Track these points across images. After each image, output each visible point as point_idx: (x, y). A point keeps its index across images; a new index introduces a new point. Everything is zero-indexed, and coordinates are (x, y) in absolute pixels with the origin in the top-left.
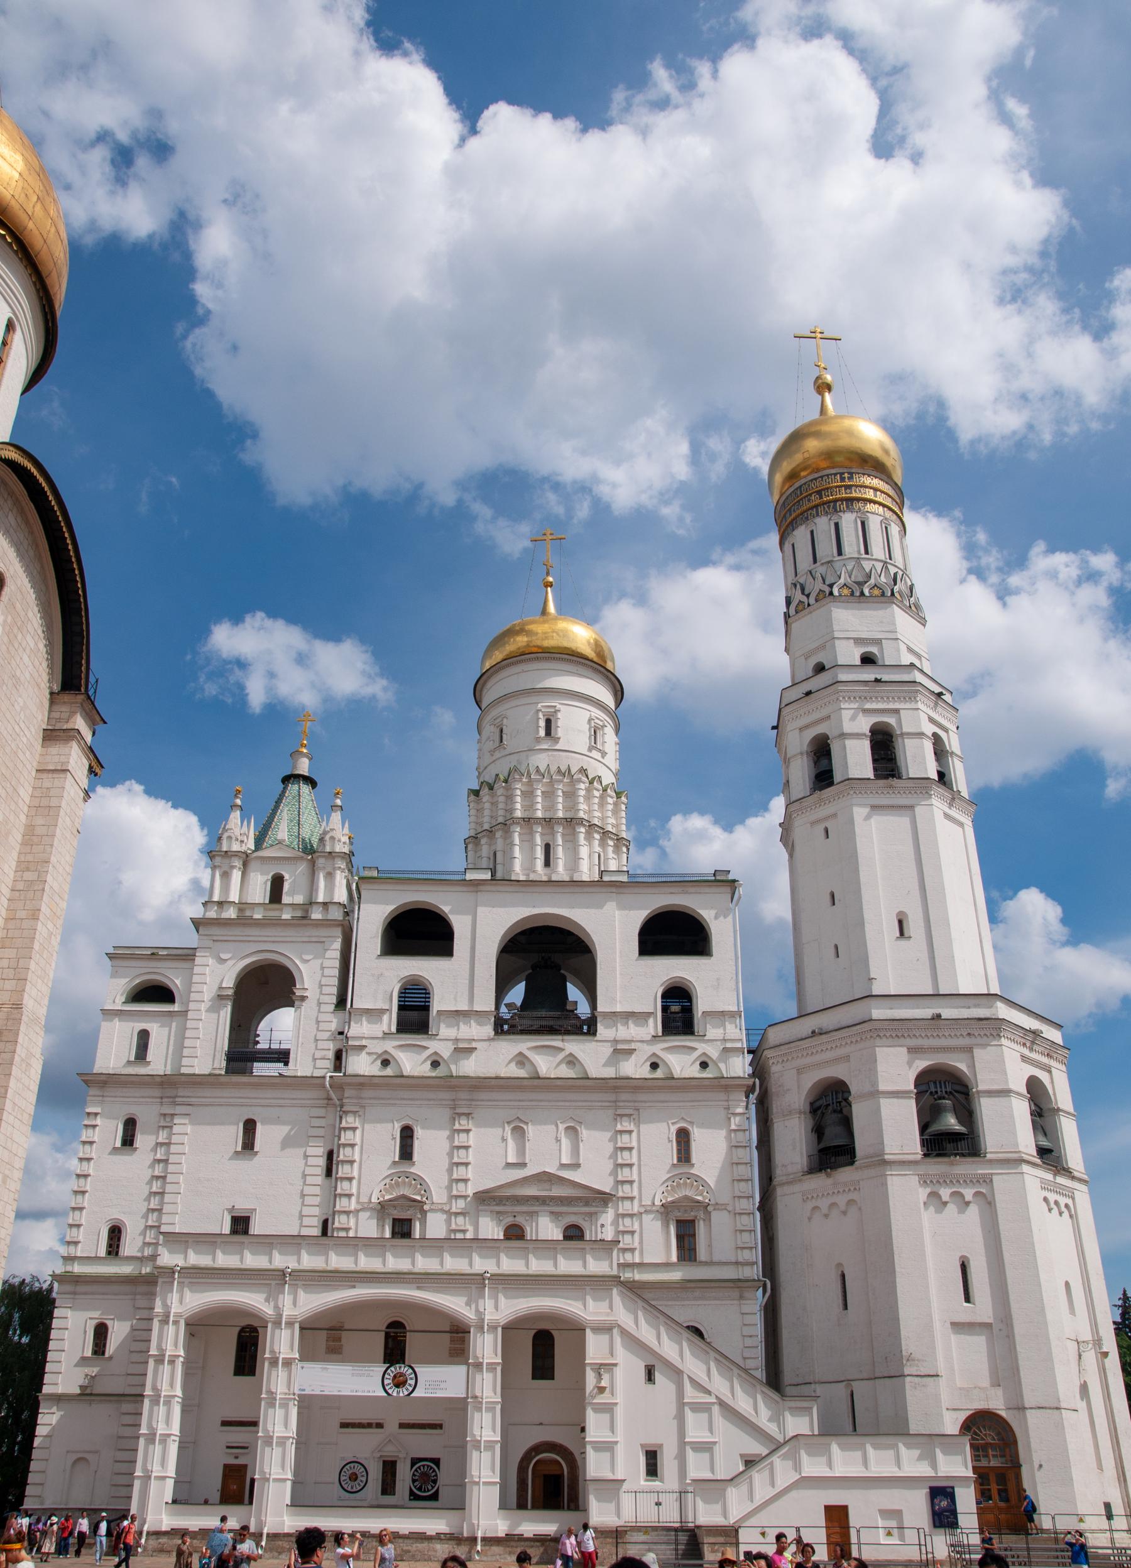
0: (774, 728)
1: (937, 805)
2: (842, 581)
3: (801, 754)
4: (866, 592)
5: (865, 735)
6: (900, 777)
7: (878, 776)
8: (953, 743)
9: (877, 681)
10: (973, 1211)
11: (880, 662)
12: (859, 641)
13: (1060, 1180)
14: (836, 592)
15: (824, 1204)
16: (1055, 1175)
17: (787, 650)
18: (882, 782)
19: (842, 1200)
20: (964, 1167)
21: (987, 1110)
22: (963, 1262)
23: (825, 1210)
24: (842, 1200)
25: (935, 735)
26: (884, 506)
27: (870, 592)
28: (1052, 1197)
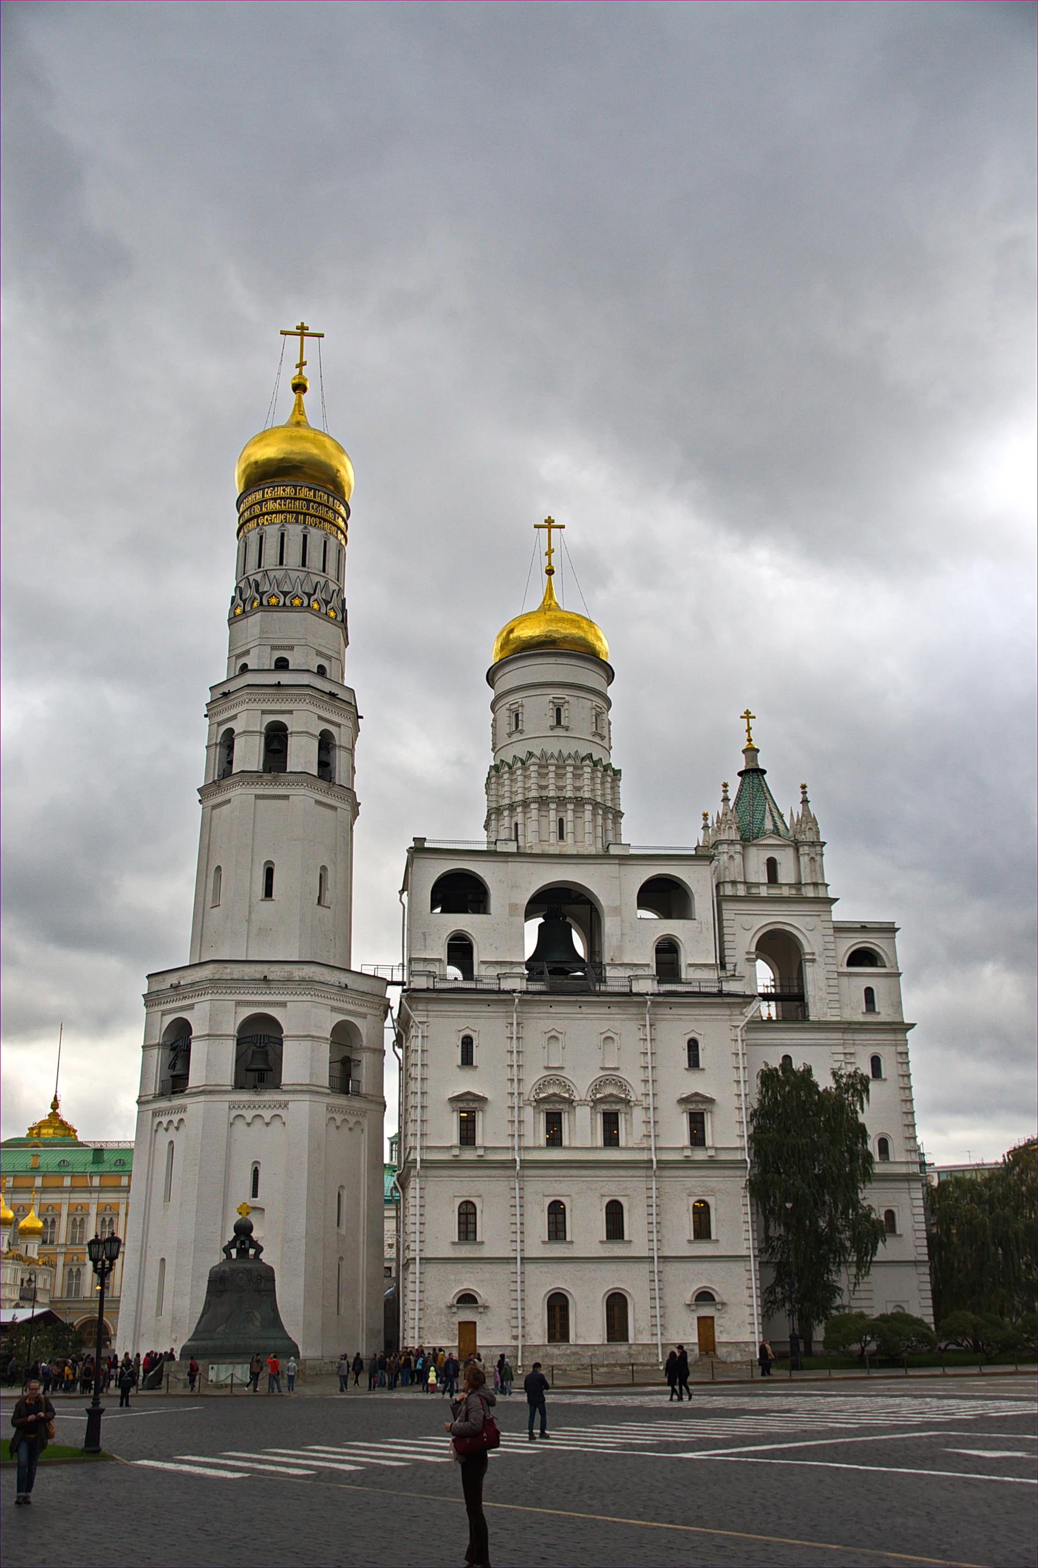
0: (206, 716)
3: (216, 744)
4: (288, 603)
5: (261, 733)
6: (284, 769)
9: (279, 685)
11: (290, 667)
12: (274, 648)
13: (357, 1103)
15: (165, 1120)
18: (267, 777)
19: (175, 1118)
22: (256, 1168)
23: (165, 1125)
24: (175, 1118)
27: (291, 602)
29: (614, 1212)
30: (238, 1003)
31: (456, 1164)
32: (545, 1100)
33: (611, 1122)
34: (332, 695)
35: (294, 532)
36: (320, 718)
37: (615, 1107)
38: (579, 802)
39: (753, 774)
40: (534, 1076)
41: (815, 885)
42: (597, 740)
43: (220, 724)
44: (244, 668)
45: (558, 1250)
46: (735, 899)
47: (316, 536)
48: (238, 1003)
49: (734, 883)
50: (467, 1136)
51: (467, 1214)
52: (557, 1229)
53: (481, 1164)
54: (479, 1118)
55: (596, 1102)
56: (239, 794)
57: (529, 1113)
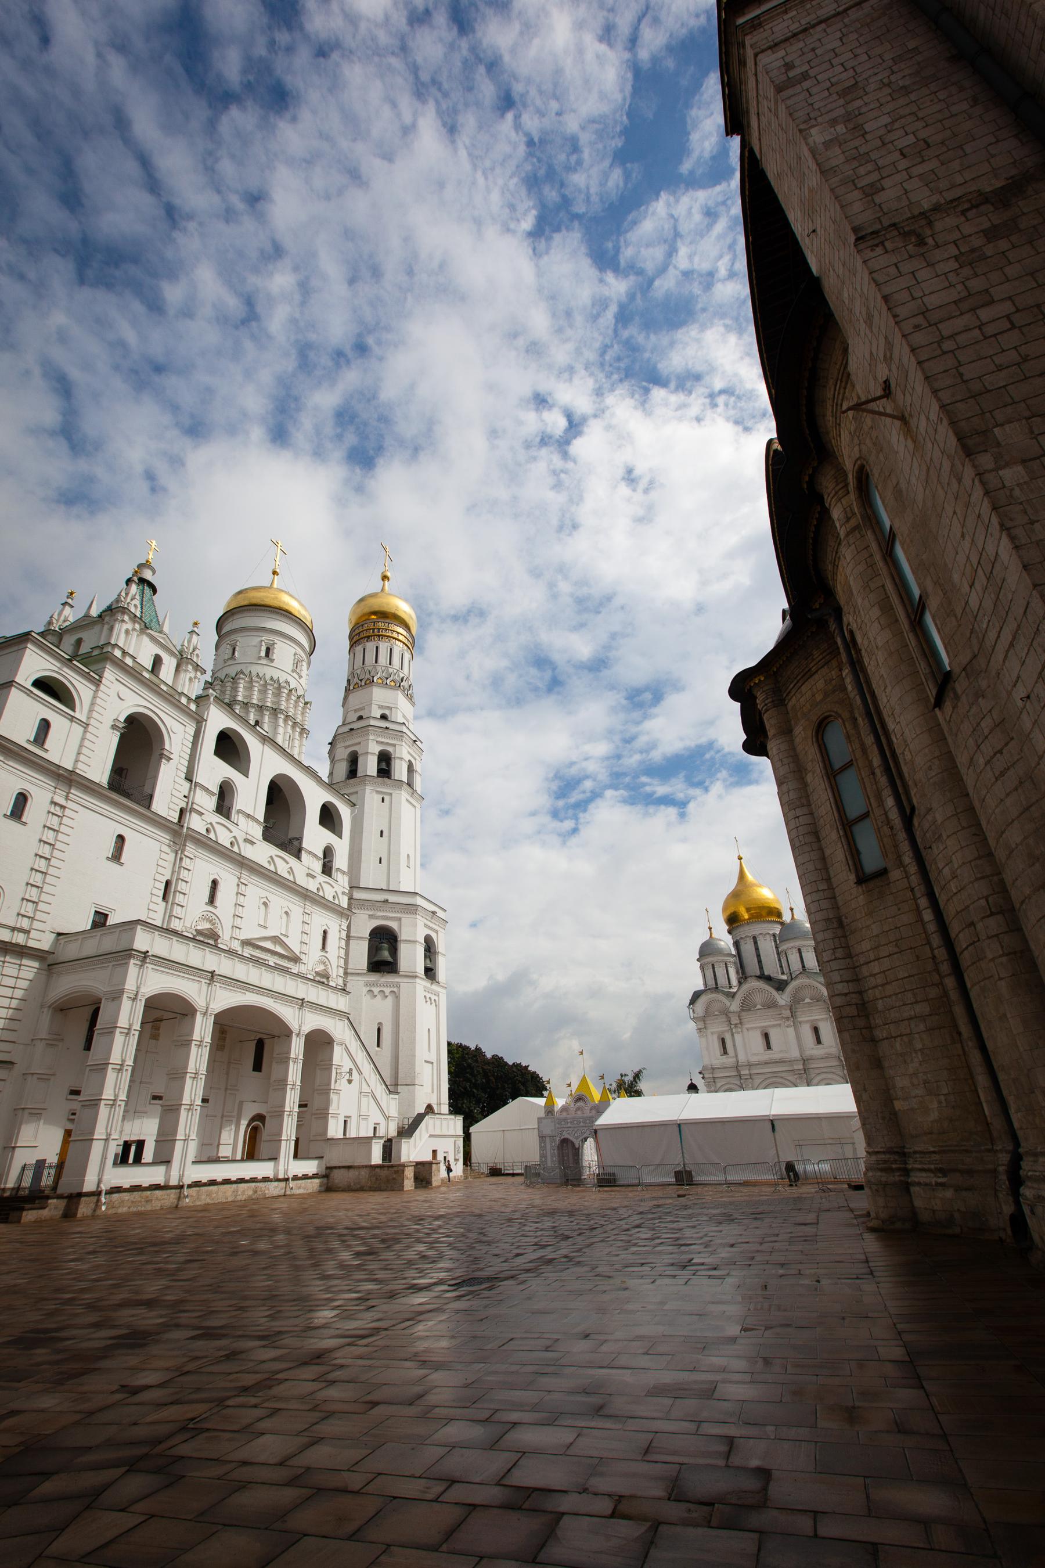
1: (404, 795)
2: (379, 675)
6: (389, 777)
7: (378, 776)
8: (418, 766)
9: (387, 728)
10: (390, 1000)
12: (380, 707)
13: (434, 987)
14: (375, 681)
16: (432, 984)
17: (343, 706)
21: (403, 949)
25: (410, 762)
26: (404, 643)
28: (428, 995)
30: (371, 917)
36: (409, 753)
43: (346, 747)
44: (360, 718)
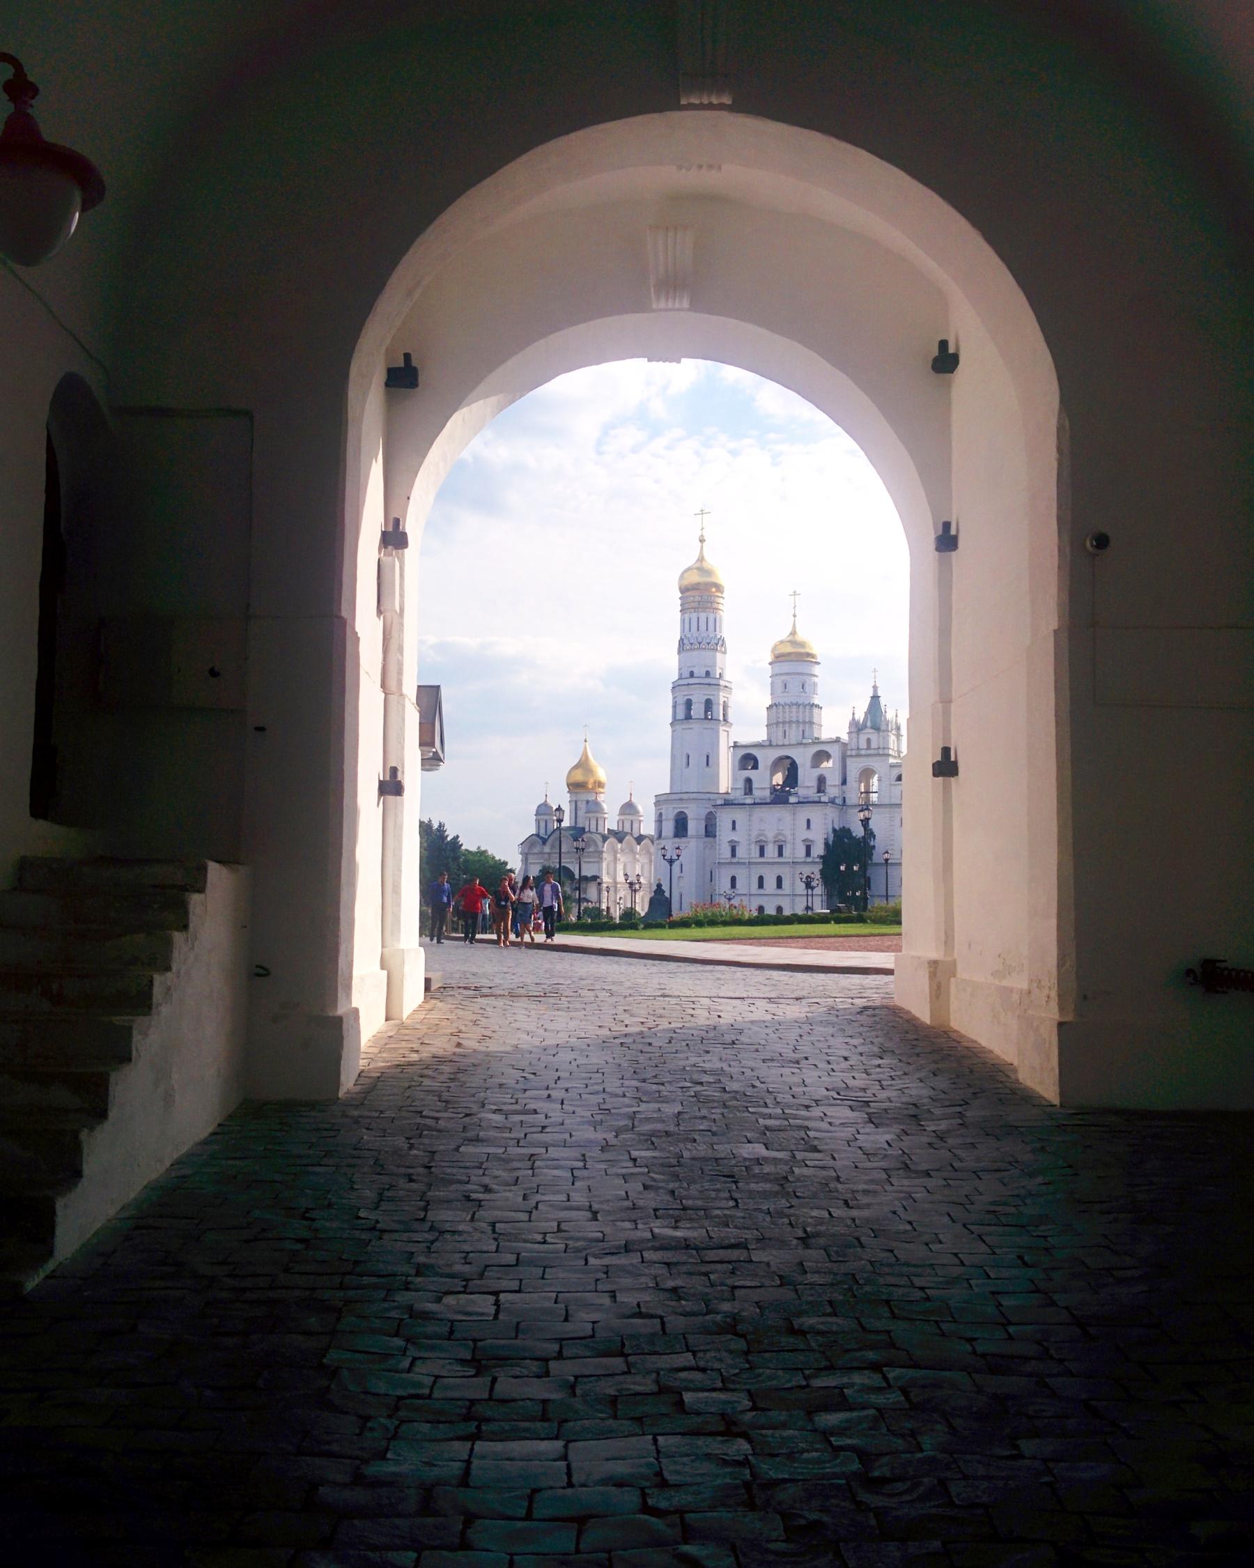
20: (684, 839)
29: (779, 880)
31: (731, 863)
32: (759, 841)
33: (780, 849)
34: (709, 684)
35: (694, 616)
37: (781, 843)
38: (790, 722)
39: (875, 698)
40: (754, 833)
41: (884, 748)
42: (804, 694)
45: (761, 891)
46: (851, 756)
47: (703, 616)
48: (674, 808)
49: (852, 750)
50: (734, 854)
51: (733, 879)
52: (761, 885)
53: (738, 863)
54: (737, 848)
55: (775, 842)
56: (678, 727)
57: (753, 845)
